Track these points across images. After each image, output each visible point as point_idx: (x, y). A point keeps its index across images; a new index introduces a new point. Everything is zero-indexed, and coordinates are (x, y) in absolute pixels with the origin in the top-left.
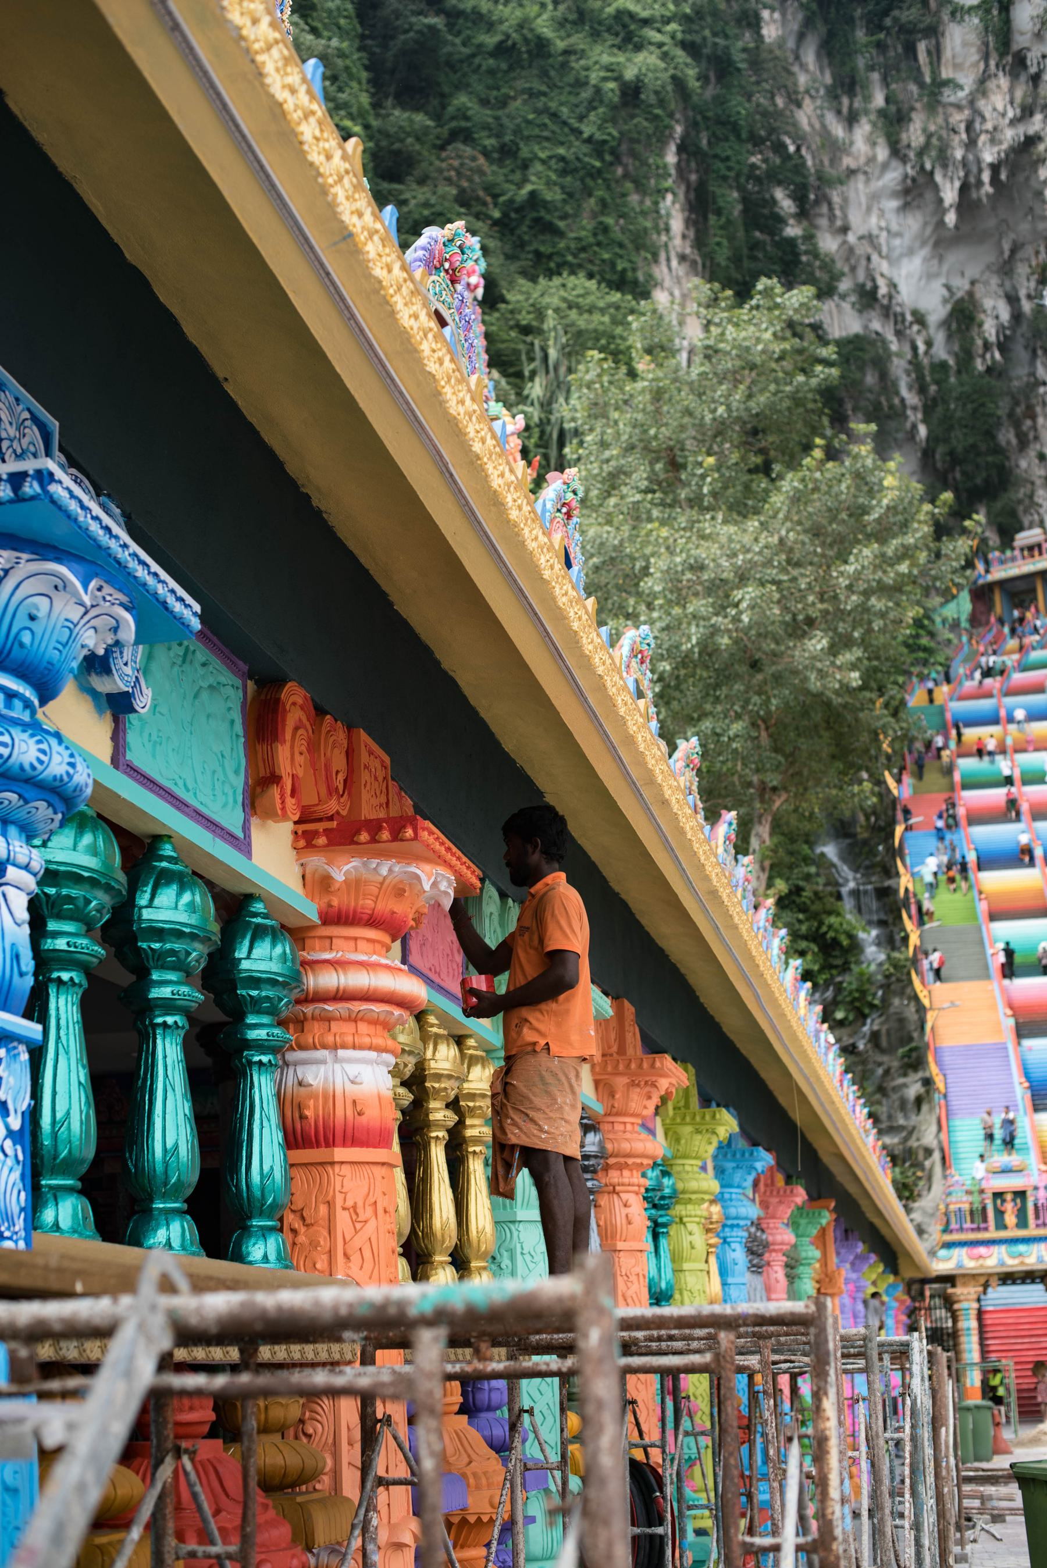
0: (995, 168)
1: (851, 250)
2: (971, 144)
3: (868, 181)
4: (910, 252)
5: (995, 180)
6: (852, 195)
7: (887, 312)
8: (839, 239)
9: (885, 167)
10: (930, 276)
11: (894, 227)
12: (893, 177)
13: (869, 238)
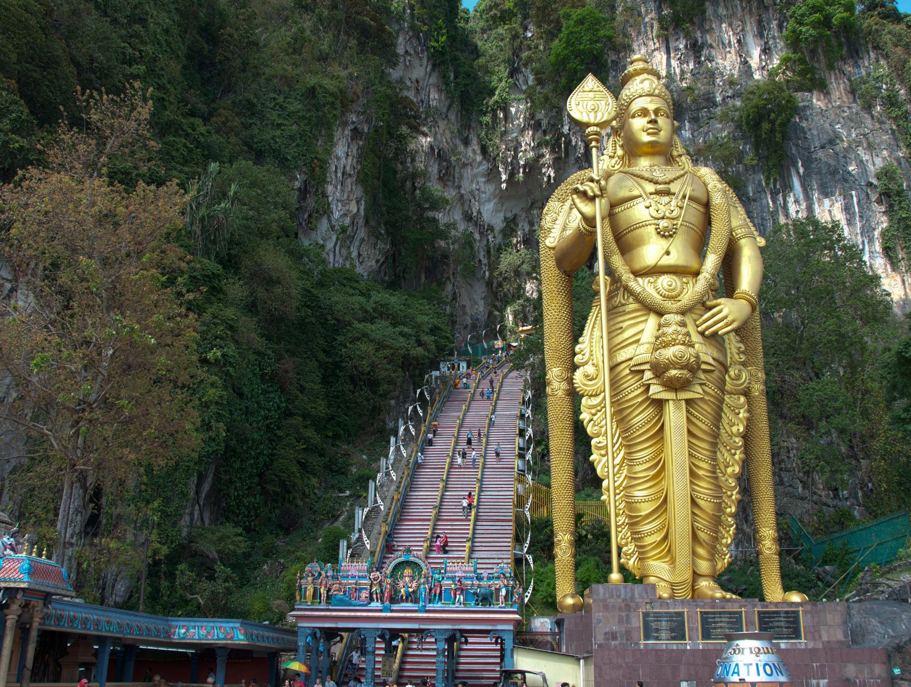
0: (524, 166)
1: (462, 196)
2: (515, 157)
3: (472, 169)
4: (489, 200)
5: (524, 172)
6: (465, 175)
7: (476, 224)
8: (457, 191)
9: (480, 163)
10: (497, 211)
11: (483, 189)
12: (485, 166)
13: (472, 192)
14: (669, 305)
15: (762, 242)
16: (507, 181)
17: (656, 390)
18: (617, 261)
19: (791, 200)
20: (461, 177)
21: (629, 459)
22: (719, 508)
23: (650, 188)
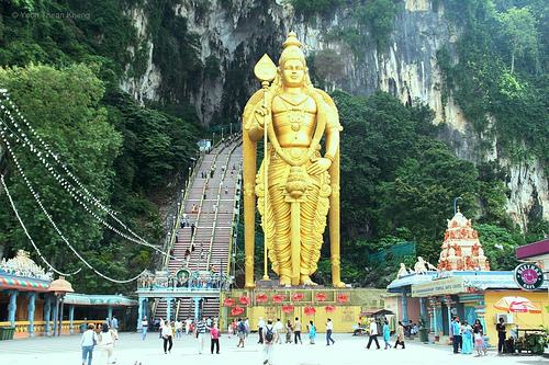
12: (223, 13)
14: (296, 162)
15: (341, 128)
16: (238, 24)
17: (288, 199)
18: (274, 139)
19: (388, 65)
20: (209, 19)
21: (276, 227)
22: (313, 247)
23: (291, 107)
